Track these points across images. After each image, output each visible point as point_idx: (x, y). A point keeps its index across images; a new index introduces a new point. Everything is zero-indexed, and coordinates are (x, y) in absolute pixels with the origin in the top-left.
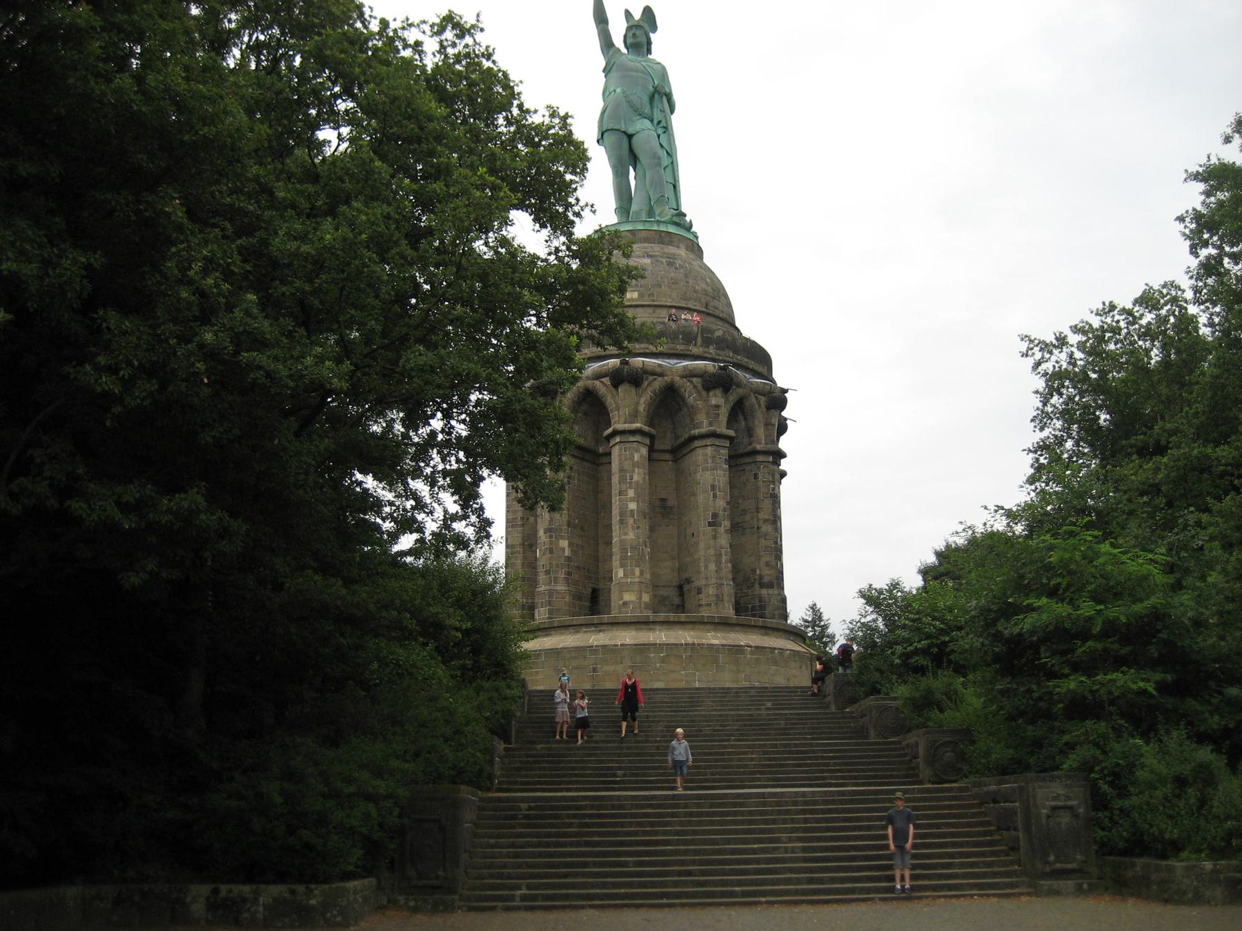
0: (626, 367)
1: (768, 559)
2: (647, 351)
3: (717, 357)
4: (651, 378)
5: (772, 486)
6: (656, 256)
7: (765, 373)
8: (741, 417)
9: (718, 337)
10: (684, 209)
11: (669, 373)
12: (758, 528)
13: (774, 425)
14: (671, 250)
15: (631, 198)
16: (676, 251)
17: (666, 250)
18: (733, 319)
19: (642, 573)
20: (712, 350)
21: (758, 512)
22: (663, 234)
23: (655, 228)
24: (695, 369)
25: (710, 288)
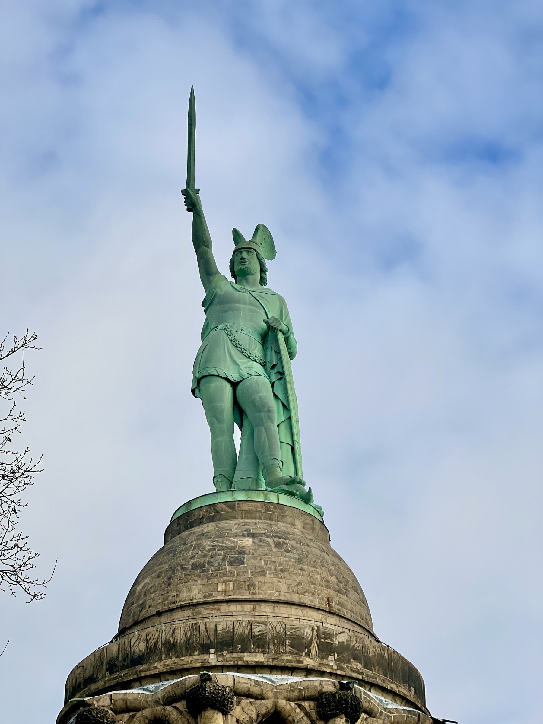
0: (208, 683)
2: (240, 663)
3: (339, 672)
4: (245, 701)
6: (261, 535)
7: (411, 696)
10: (304, 476)
14: (281, 526)
15: (235, 463)
16: (291, 529)
17: (275, 528)
18: (368, 620)
20: (331, 661)
23: (261, 499)
24: (306, 688)
25: (333, 578)
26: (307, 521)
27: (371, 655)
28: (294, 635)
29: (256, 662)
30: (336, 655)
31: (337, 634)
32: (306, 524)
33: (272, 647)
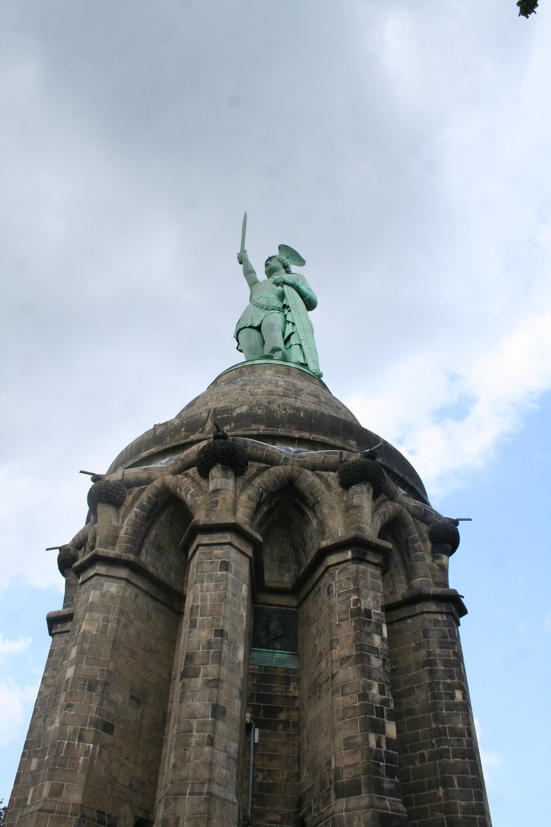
1: (349, 733)
4: (136, 490)
5: (354, 597)
8: (309, 513)
9: (241, 415)
11: (158, 474)
12: (333, 676)
13: (358, 507)
19: (56, 792)
21: (332, 648)
22: (244, 369)
26: (280, 370)
27: (278, 416)
28: (189, 422)
29: (149, 453)
30: (233, 425)
31: (235, 408)
32: (278, 371)
33: (168, 439)
